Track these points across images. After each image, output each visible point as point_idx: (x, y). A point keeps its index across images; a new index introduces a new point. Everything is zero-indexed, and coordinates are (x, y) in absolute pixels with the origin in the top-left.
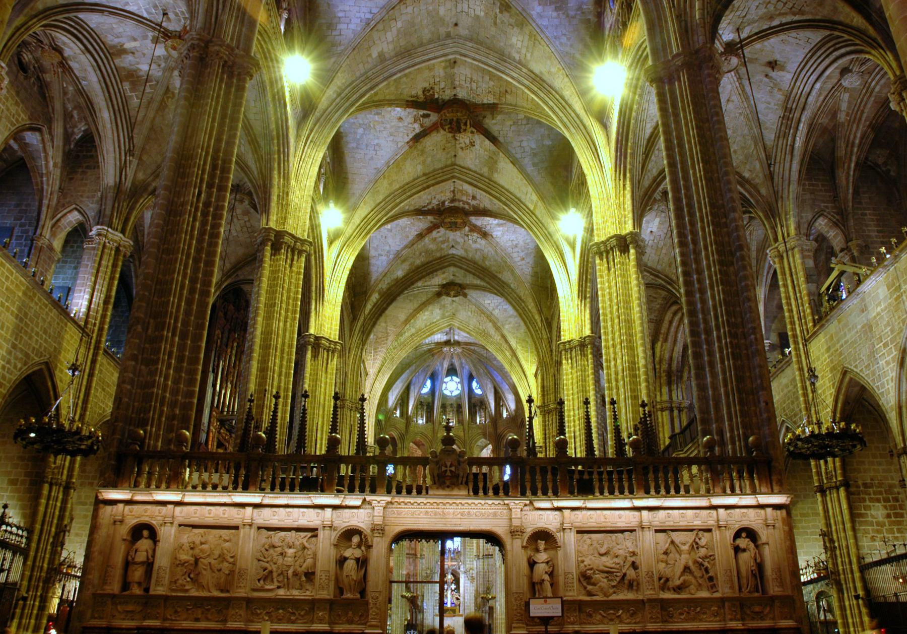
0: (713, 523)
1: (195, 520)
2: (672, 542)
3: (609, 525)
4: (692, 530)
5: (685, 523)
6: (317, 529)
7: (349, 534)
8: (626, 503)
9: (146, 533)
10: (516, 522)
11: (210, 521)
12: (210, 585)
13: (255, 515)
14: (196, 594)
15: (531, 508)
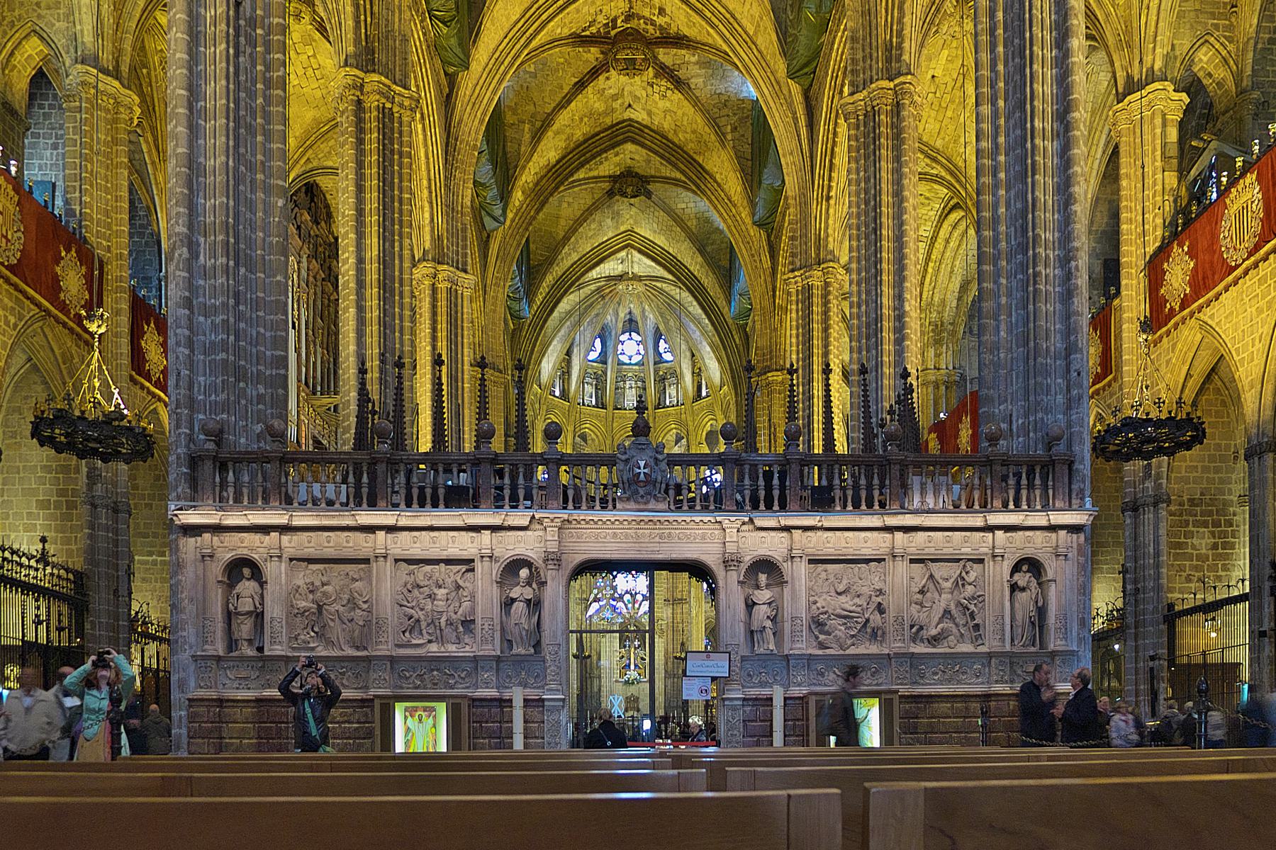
0: (986, 550)
1: (310, 552)
2: (931, 576)
3: (850, 553)
4: (958, 560)
5: (951, 551)
6: (473, 561)
7: (515, 565)
8: (875, 521)
9: (246, 572)
10: (731, 548)
11: (329, 553)
12: (342, 641)
13: (389, 542)
14: (324, 653)
15: (751, 527)
